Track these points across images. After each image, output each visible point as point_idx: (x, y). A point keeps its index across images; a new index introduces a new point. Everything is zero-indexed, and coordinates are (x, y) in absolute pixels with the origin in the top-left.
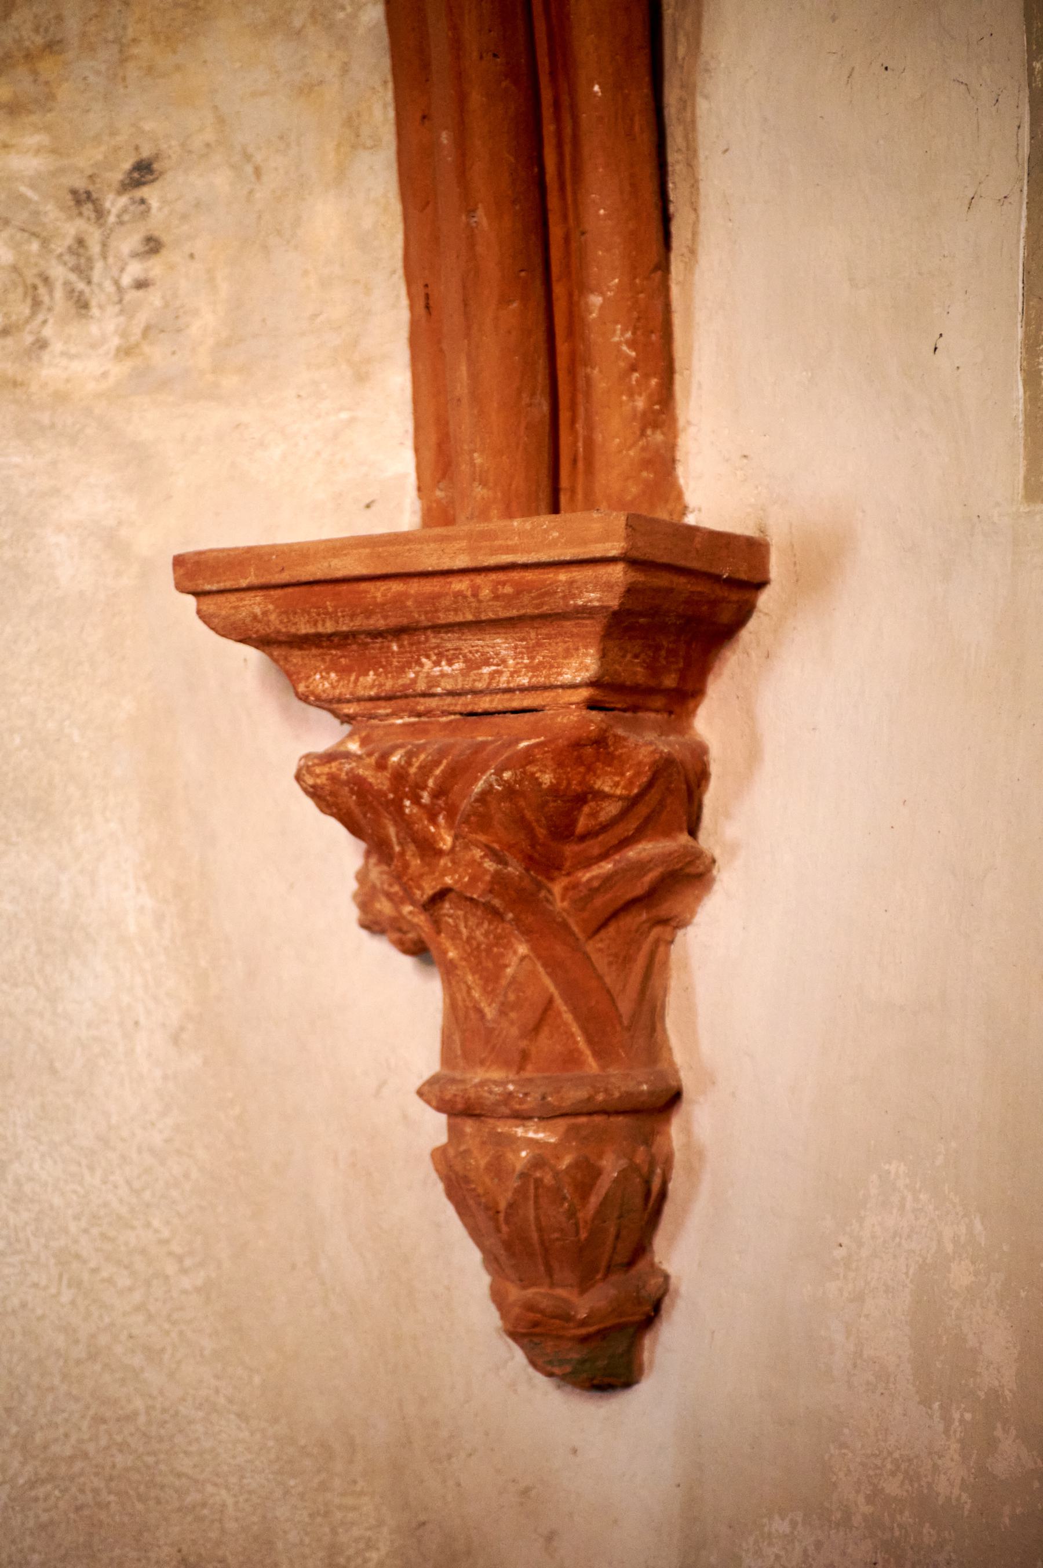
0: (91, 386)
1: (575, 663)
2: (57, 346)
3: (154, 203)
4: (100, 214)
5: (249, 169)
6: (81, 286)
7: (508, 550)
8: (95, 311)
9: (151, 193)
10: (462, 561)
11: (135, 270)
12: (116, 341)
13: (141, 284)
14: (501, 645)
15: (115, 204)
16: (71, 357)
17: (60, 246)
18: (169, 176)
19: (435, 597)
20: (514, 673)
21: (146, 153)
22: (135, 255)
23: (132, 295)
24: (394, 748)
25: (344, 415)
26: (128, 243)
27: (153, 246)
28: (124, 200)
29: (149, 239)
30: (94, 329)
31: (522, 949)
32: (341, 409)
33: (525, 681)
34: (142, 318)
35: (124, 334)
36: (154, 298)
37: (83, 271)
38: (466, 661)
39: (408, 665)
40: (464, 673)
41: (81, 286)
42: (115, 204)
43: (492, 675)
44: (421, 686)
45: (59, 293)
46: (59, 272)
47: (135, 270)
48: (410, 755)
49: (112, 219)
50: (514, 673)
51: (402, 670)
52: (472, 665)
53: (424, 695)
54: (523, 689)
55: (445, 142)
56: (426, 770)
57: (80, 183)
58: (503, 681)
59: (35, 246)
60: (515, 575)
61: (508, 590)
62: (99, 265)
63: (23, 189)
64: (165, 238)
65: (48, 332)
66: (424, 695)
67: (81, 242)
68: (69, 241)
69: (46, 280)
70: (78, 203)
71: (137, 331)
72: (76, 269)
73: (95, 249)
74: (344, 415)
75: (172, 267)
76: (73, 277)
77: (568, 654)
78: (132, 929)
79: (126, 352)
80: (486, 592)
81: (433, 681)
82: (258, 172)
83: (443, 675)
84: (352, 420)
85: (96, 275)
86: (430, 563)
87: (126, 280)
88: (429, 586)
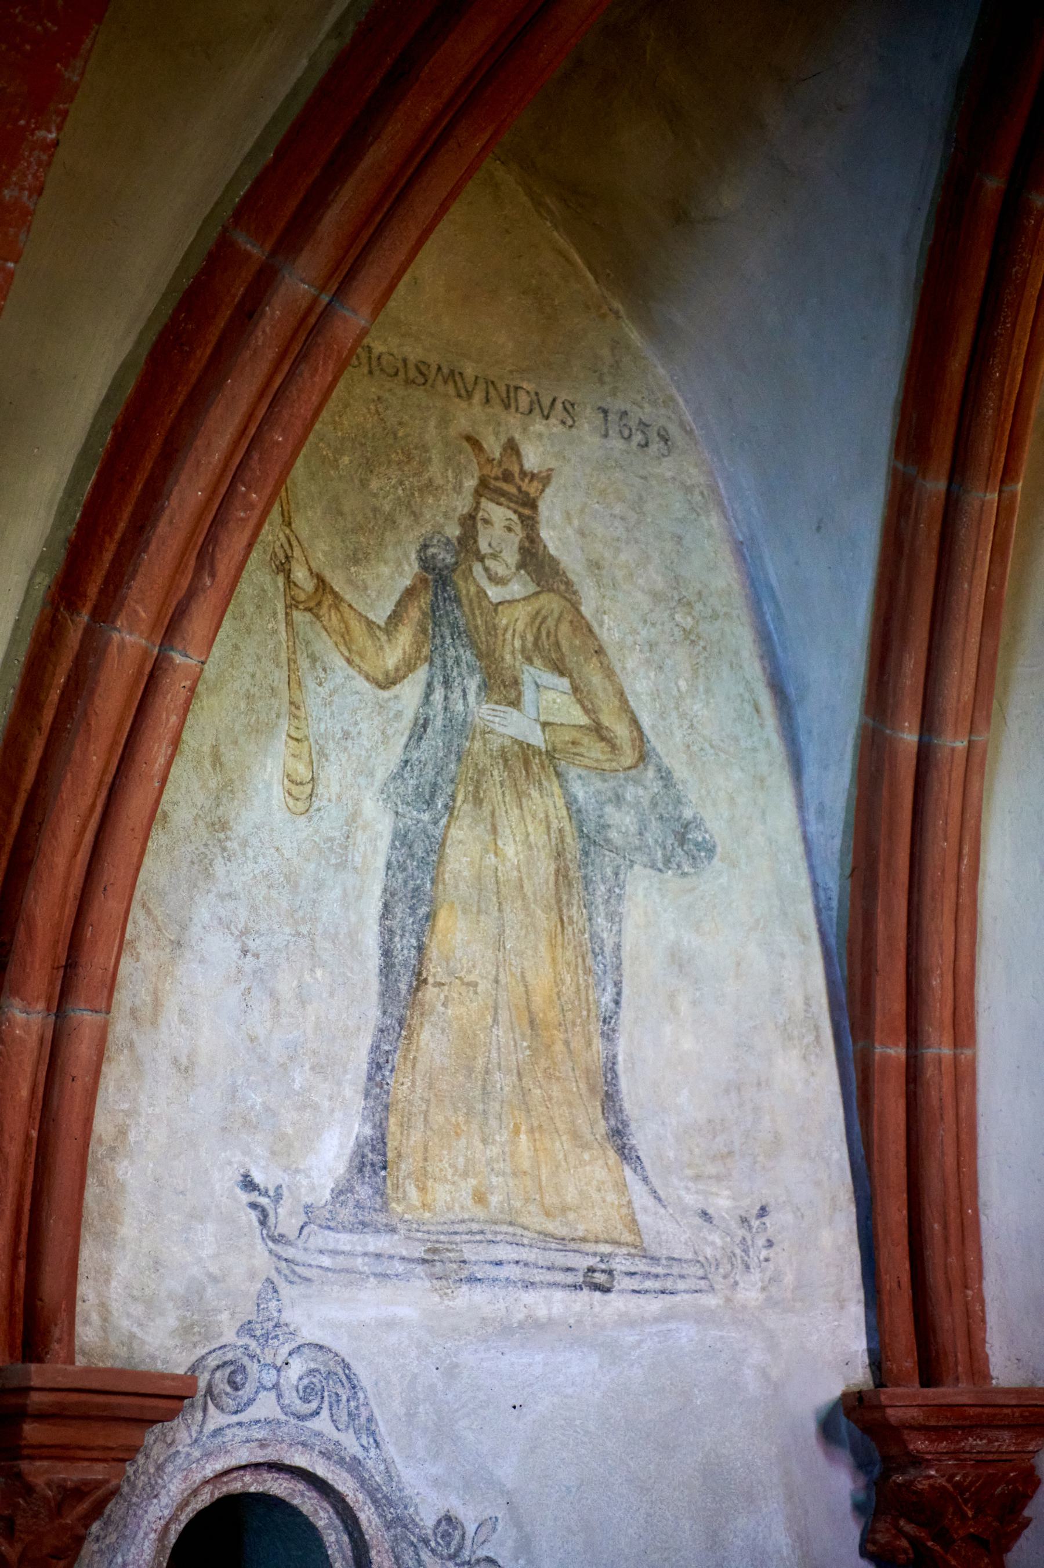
0: (753, 1303)
1: (1034, 1443)
2: (741, 1285)
3: (768, 1225)
4: (750, 1228)
5: (799, 1214)
6: (746, 1258)
7: (1036, 1399)
8: (752, 1270)
9: (766, 1220)
10: (1014, 1402)
11: (764, 1253)
12: (760, 1284)
13: (767, 1260)
14: (1006, 1435)
15: (755, 1223)
16: (746, 1290)
17: (738, 1240)
18: (772, 1213)
19: (995, 1415)
20: (1009, 1446)
21: (764, 1203)
22: (765, 1247)
23: (764, 1264)
24: (957, 1474)
25: (836, 1323)
26: (761, 1242)
27: (770, 1244)
28: (758, 1222)
29: (769, 1241)
30: (752, 1278)
31: (986, 1560)
32: (835, 1320)
33: (1013, 1449)
34: (768, 1274)
35: (762, 1281)
36: (771, 1265)
37: (746, 1251)
38: (989, 1439)
39: (962, 1440)
40: (987, 1444)
41: (746, 1258)
42: (755, 1223)
43: (999, 1446)
44: (967, 1449)
45: (739, 1261)
46: (738, 1251)
47: (764, 1253)
48: (965, 1476)
49: (754, 1230)
50: (1009, 1446)
51: (959, 1442)
52: (990, 1441)
53: (968, 1452)
54: (1011, 1452)
55: (936, 1226)
56: (972, 1483)
57: (744, 1214)
58: (1004, 1448)
59: (728, 1239)
60: (1031, 1409)
61: (1027, 1414)
62: (751, 1250)
63: (724, 1214)
64: (774, 1241)
65: (738, 1278)
66: (968, 1452)
67: (744, 1239)
68: (740, 1238)
69: (734, 1255)
70: (743, 1222)
71: (767, 1279)
72: (744, 1251)
73: (750, 1243)
74: (836, 1323)
75: (777, 1254)
76: (743, 1254)
77: (1032, 1440)
78: (785, 1555)
79: (763, 1289)
80: (1017, 1414)
81: (972, 1447)
82: (802, 1216)
83: (977, 1445)
84: (839, 1326)
85: (751, 1254)
86: (1001, 1402)
87: (762, 1258)
88: (997, 1410)
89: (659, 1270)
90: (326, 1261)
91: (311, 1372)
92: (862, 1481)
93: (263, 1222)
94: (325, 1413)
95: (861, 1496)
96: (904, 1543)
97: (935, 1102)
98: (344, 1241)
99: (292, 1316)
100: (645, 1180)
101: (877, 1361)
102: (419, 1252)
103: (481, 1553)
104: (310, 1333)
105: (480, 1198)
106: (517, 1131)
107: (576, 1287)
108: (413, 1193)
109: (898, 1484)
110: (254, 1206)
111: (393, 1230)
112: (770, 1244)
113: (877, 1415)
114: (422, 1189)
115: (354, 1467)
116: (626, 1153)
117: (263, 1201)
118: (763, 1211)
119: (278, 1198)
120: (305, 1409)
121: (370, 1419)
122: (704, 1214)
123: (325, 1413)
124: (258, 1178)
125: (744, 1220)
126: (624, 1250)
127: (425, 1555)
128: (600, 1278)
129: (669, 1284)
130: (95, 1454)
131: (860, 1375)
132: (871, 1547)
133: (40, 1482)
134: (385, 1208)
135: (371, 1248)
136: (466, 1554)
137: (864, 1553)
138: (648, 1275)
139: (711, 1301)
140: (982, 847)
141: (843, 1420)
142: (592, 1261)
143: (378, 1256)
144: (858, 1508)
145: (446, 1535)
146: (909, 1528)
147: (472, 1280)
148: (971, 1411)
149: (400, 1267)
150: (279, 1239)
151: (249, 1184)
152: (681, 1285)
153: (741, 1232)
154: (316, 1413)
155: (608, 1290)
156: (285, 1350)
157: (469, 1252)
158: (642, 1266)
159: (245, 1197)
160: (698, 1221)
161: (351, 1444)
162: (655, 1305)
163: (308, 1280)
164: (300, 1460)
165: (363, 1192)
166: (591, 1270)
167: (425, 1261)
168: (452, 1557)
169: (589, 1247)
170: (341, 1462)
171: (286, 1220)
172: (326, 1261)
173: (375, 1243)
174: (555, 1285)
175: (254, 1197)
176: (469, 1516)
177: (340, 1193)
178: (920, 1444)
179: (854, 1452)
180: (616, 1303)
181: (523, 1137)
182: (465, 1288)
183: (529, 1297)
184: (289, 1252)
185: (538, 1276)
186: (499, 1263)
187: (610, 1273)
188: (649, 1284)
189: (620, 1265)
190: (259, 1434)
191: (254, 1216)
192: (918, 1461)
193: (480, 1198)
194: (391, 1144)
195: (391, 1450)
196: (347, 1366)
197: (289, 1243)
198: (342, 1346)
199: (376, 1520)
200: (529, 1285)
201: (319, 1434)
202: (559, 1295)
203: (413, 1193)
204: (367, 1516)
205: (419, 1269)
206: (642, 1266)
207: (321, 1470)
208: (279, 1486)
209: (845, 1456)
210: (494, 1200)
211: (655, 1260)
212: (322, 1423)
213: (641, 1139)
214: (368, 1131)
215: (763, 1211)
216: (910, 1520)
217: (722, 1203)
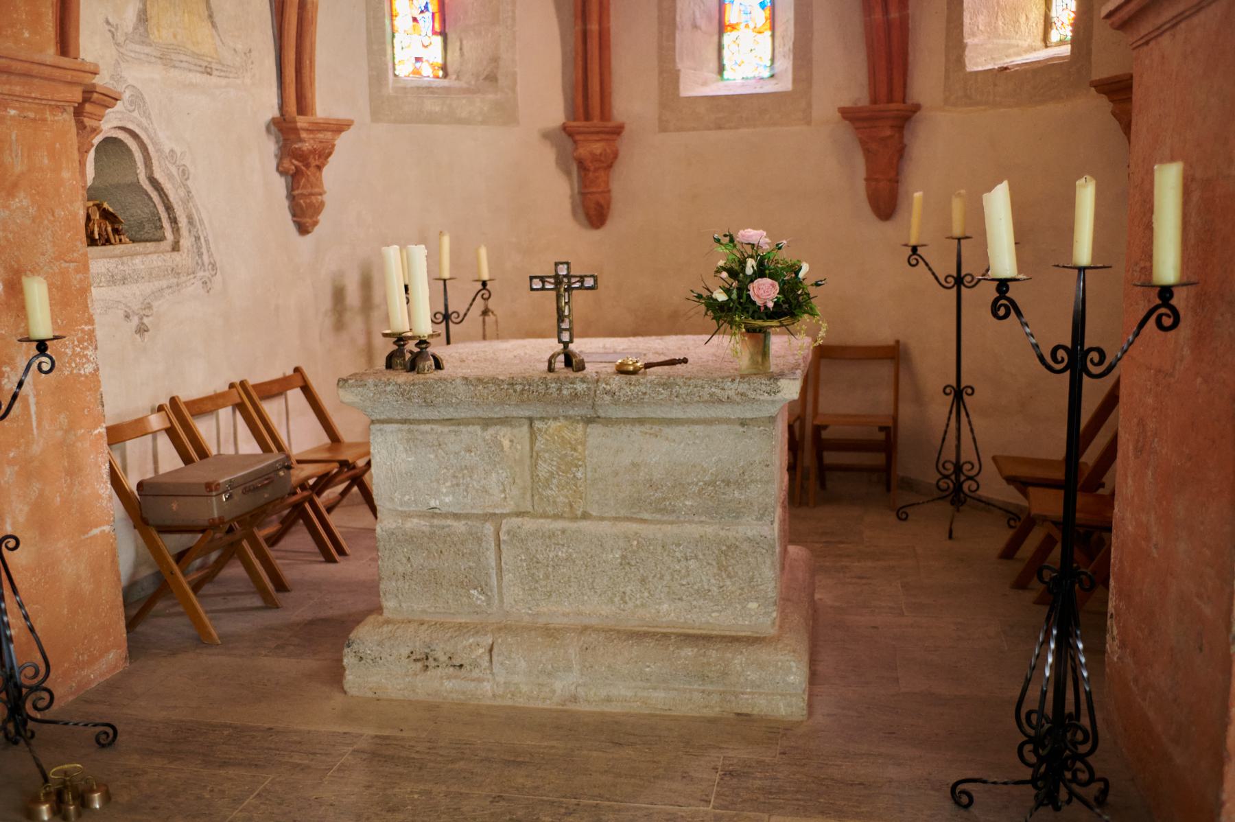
14: (330, 133)
26: (250, 62)
42: (248, 55)
89: (224, 69)
90: (133, 55)
91: (132, 95)
92: (277, 146)
93: (113, 37)
94: (136, 111)
95: (277, 152)
96: (293, 167)
97: (310, 17)
98: (138, 48)
99: (125, 74)
100: (219, 35)
101: (282, 107)
102: (159, 54)
103: (183, 163)
104: (130, 81)
105: (175, 36)
106: (184, 12)
107: (203, 73)
108: (156, 33)
109: (296, 149)
110: (110, 31)
111: (151, 45)
112: (252, 63)
113: (292, 125)
114: (158, 31)
115: (145, 130)
116: (214, 25)
117: (113, 29)
118: (250, 51)
119: (117, 29)
120: (131, 108)
121: (149, 114)
122: (235, 50)
123: (136, 111)
124: (111, 20)
125: (245, 54)
126: (214, 61)
127: (167, 162)
128: (209, 70)
129: (227, 74)
130: (94, 117)
131: (275, 113)
132: (280, 169)
133: (87, 124)
134: (148, 37)
135: (146, 51)
136: (178, 162)
137: (278, 170)
138: (222, 71)
139: (239, 81)
140: (911, 58)
141: (273, 128)
142: (206, 64)
143: (147, 55)
144: (276, 156)
145: (172, 156)
146: (296, 162)
147: (175, 67)
148: (322, 125)
149: (153, 59)
150: (118, 45)
151: (108, 22)
152: (231, 75)
153: (245, 58)
154: (134, 110)
155: (211, 75)
156: (124, 86)
157: (174, 57)
158: (219, 67)
159: (107, 27)
160: (233, 52)
161: (144, 122)
162: (224, 82)
163: (128, 61)
164: (130, 126)
165: (142, 30)
166: (206, 67)
167: (161, 58)
168: (174, 163)
169: (205, 58)
170: (142, 128)
171: (121, 39)
172: (133, 55)
173: (147, 50)
174: (197, 71)
175: (109, 27)
176: (178, 150)
177: (135, 28)
178: (304, 135)
179: (276, 137)
180: (213, 80)
181: (186, 15)
182: (173, 69)
183: (191, 75)
184: (121, 50)
185: (193, 67)
186: (182, 61)
187: (211, 68)
188: (222, 74)
189: (214, 66)
190: (119, 116)
191: (109, 35)
192: (301, 140)
193: (175, 36)
194: (148, 13)
195: (156, 126)
196: (142, 95)
197: (121, 46)
198: (139, 86)
199: (153, 149)
200: (190, 70)
201: (135, 118)
202: (198, 75)
203: (156, 33)
204: (151, 148)
205: (159, 61)
206: (219, 67)
207: (137, 131)
208: (122, 135)
209: (273, 139)
210: (179, 37)
211: (223, 65)
212: (136, 114)
213: (217, 19)
214: (141, 6)
215: (250, 51)
216: (297, 160)
217: (239, 47)
